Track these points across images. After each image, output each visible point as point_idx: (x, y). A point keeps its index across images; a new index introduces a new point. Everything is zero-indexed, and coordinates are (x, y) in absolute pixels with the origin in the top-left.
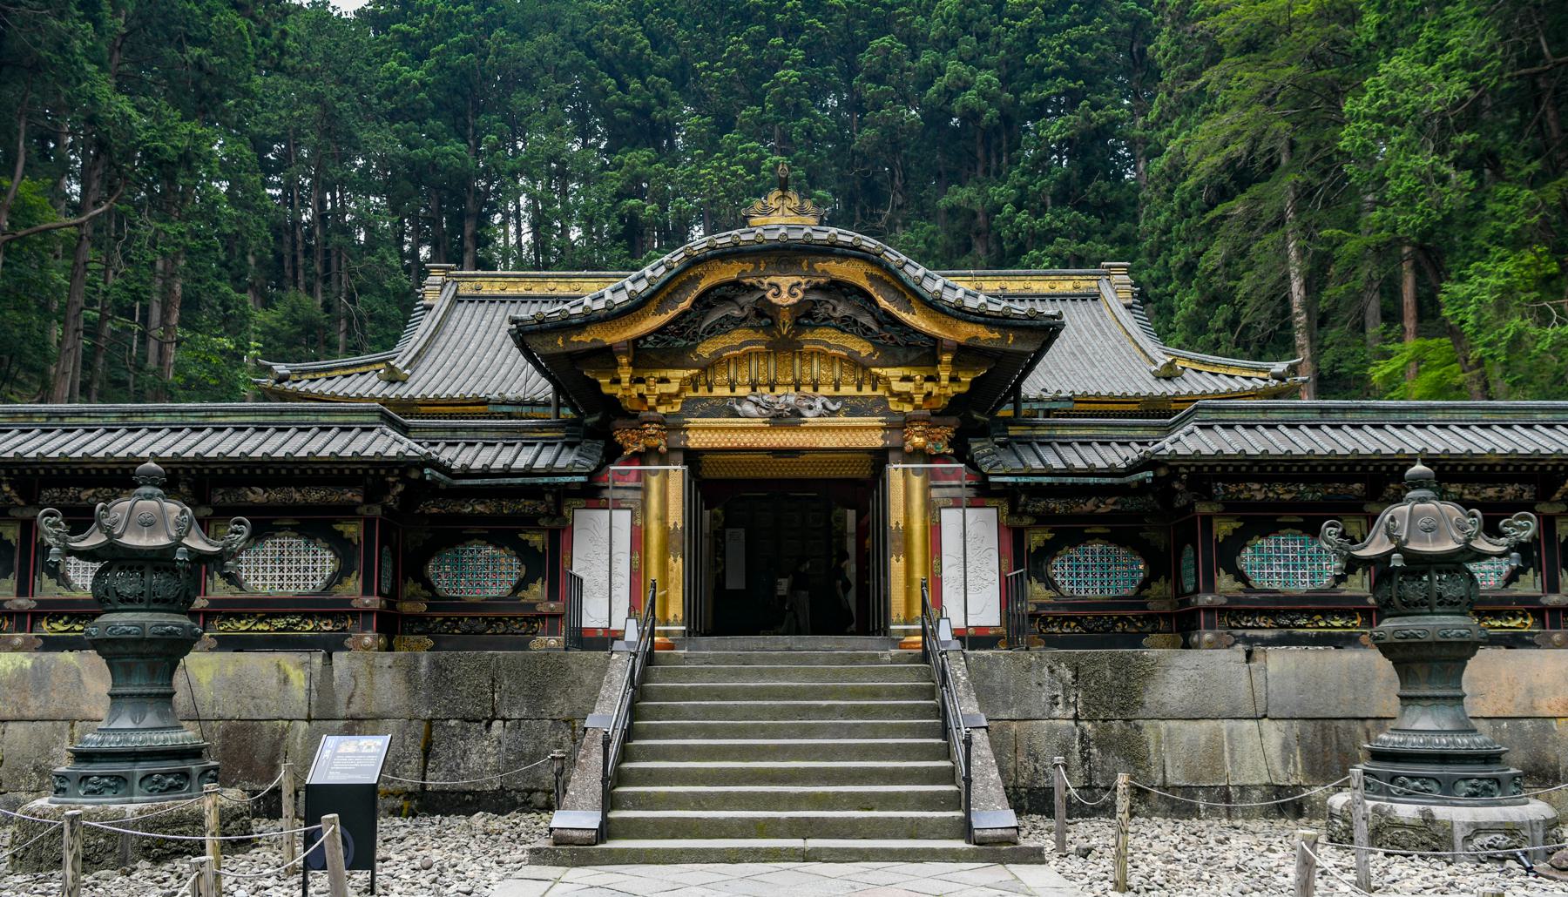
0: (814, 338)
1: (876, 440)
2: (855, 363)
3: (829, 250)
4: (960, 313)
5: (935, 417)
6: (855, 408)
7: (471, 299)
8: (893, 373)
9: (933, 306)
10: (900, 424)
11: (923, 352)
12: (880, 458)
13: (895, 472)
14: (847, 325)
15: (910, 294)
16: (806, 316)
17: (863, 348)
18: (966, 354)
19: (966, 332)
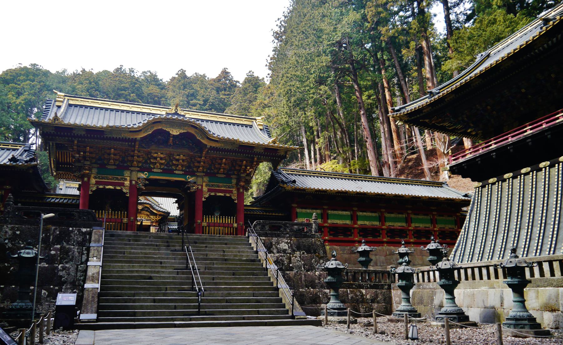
0: (143, 212)
1: (149, 224)
2: (147, 215)
3: (146, 203)
4: (159, 211)
5: (157, 222)
6: (147, 220)
7: (69, 187)
8: (152, 216)
9: (157, 210)
10: (152, 222)
11: (156, 215)
12: (149, 226)
13: (151, 227)
14: (147, 211)
15: (154, 209)
16: (142, 210)
17: (148, 214)
18: (160, 215)
19: (160, 213)
